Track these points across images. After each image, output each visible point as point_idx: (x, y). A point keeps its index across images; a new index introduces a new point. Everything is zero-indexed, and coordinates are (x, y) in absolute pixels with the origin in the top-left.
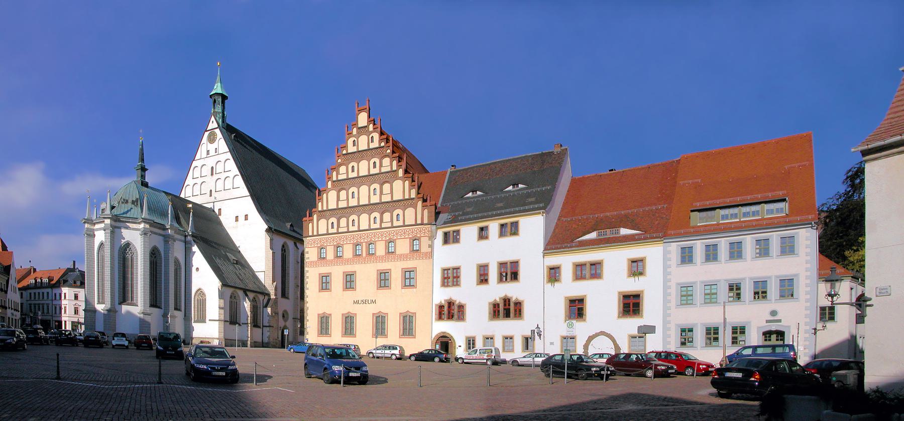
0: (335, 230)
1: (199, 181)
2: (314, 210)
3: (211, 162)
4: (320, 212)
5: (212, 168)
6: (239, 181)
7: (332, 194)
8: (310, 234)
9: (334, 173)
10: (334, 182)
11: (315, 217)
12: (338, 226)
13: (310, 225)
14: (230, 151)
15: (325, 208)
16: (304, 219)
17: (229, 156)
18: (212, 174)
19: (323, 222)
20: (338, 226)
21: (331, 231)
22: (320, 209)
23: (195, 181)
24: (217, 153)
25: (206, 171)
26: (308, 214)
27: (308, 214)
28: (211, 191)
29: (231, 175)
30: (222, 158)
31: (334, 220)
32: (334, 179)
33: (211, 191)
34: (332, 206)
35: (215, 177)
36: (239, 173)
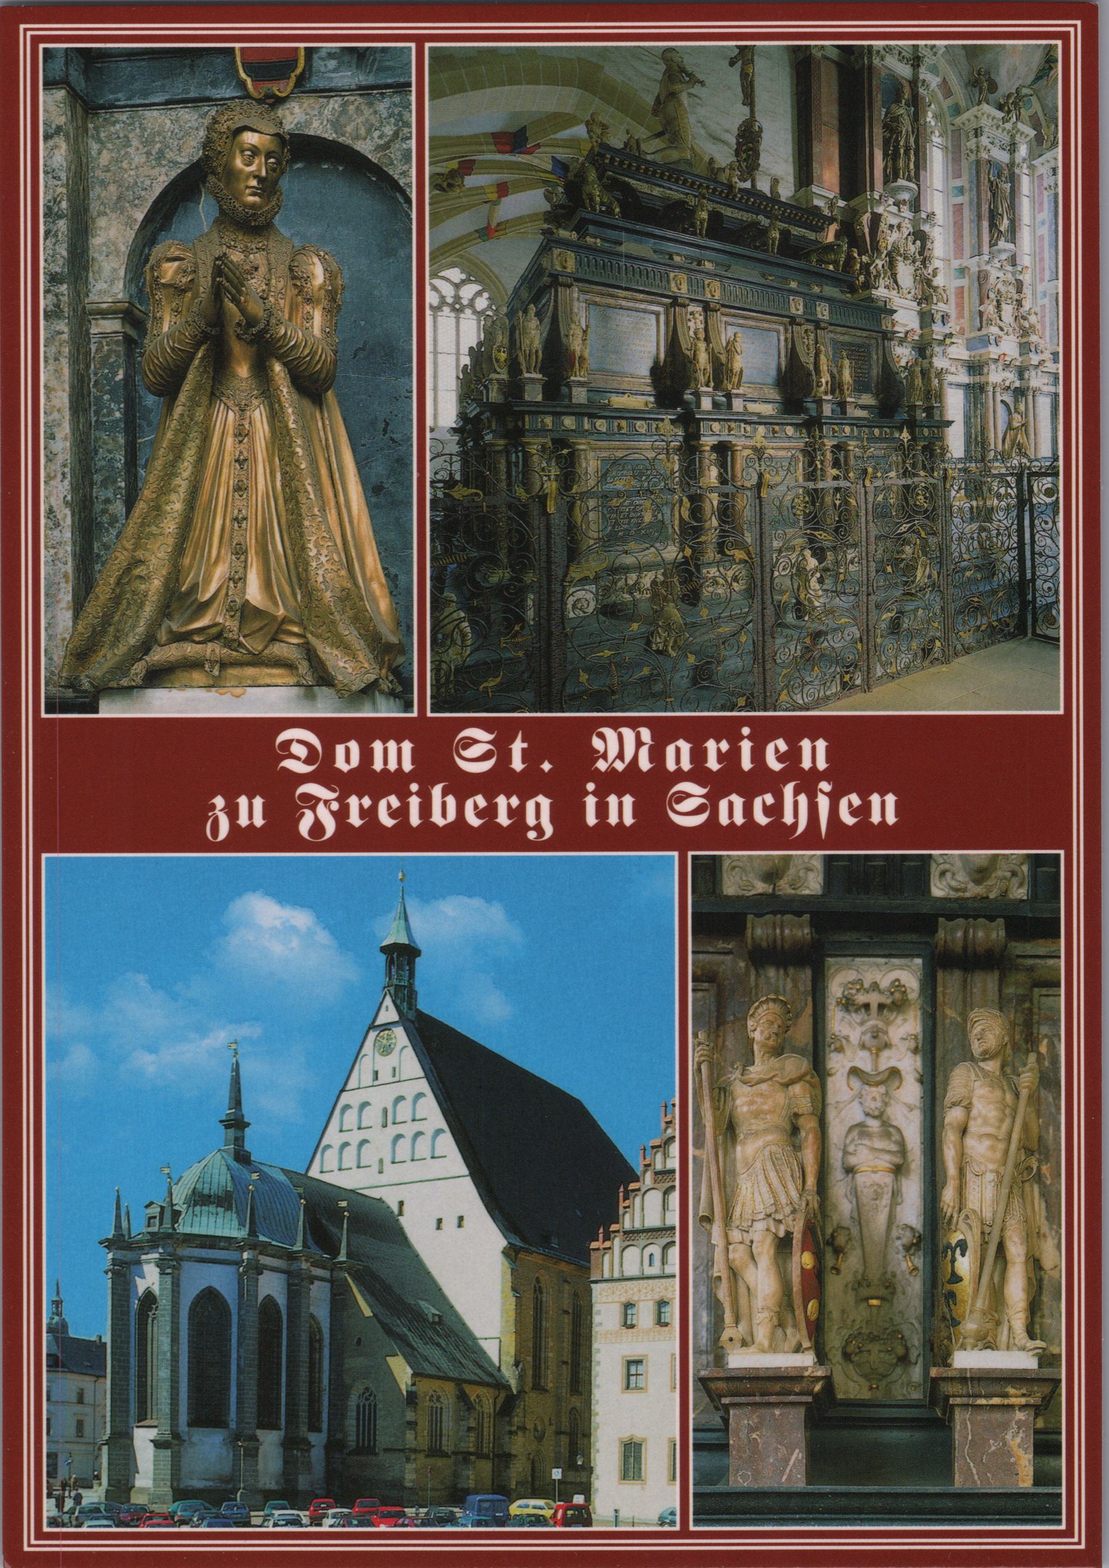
0: (655, 1270)
1: (355, 1138)
2: (614, 1227)
3: (380, 1098)
4: (625, 1233)
5: (385, 1111)
6: (447, 1144)
7: (654, 1199)
8: (606, 1275)
9: (659, 1156)
10: (657, 1173)
11: (617, 1243)
12: (664, 1262)
13: (607, 1258)
14: (427, 1077)
15: (638, 1225)
16: (594, 1245)
17: (424, 1086)
18: (385, 1126)
19: (632, 1254)
20: (664, 1262)
21: (649, 1271)
22: (627, 1226)
23: (345, 1137)
24: (396, 1079)
25: (372, 1116)
26: (601, 1236)
27: (601, 1236)
28: (381, 1161)
29: (429, 1128)
30: (409, 1090)
31: (656, 1250)
32: (659, 1167)
33: (381, 1161)
34: (653, 1220)
35: (392, 1131)
36: (446, 1127)
